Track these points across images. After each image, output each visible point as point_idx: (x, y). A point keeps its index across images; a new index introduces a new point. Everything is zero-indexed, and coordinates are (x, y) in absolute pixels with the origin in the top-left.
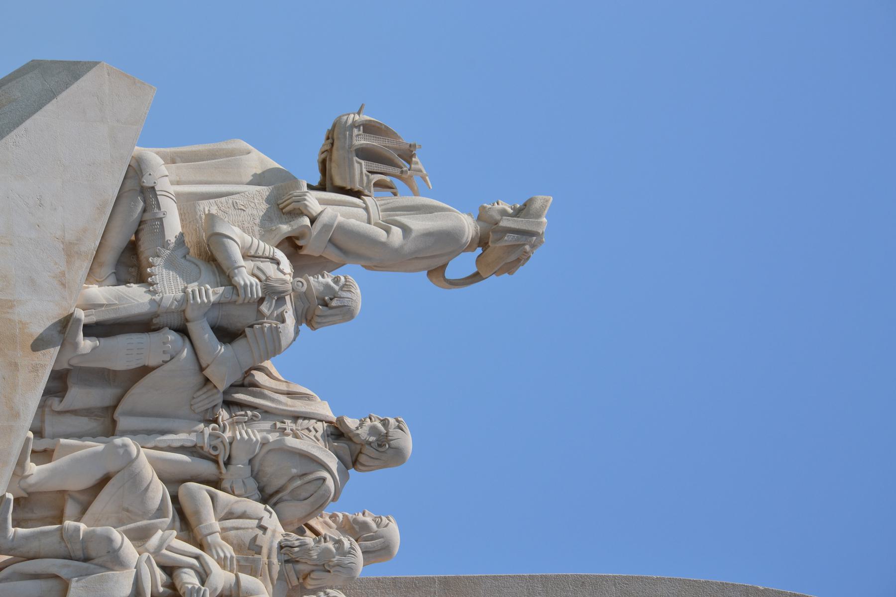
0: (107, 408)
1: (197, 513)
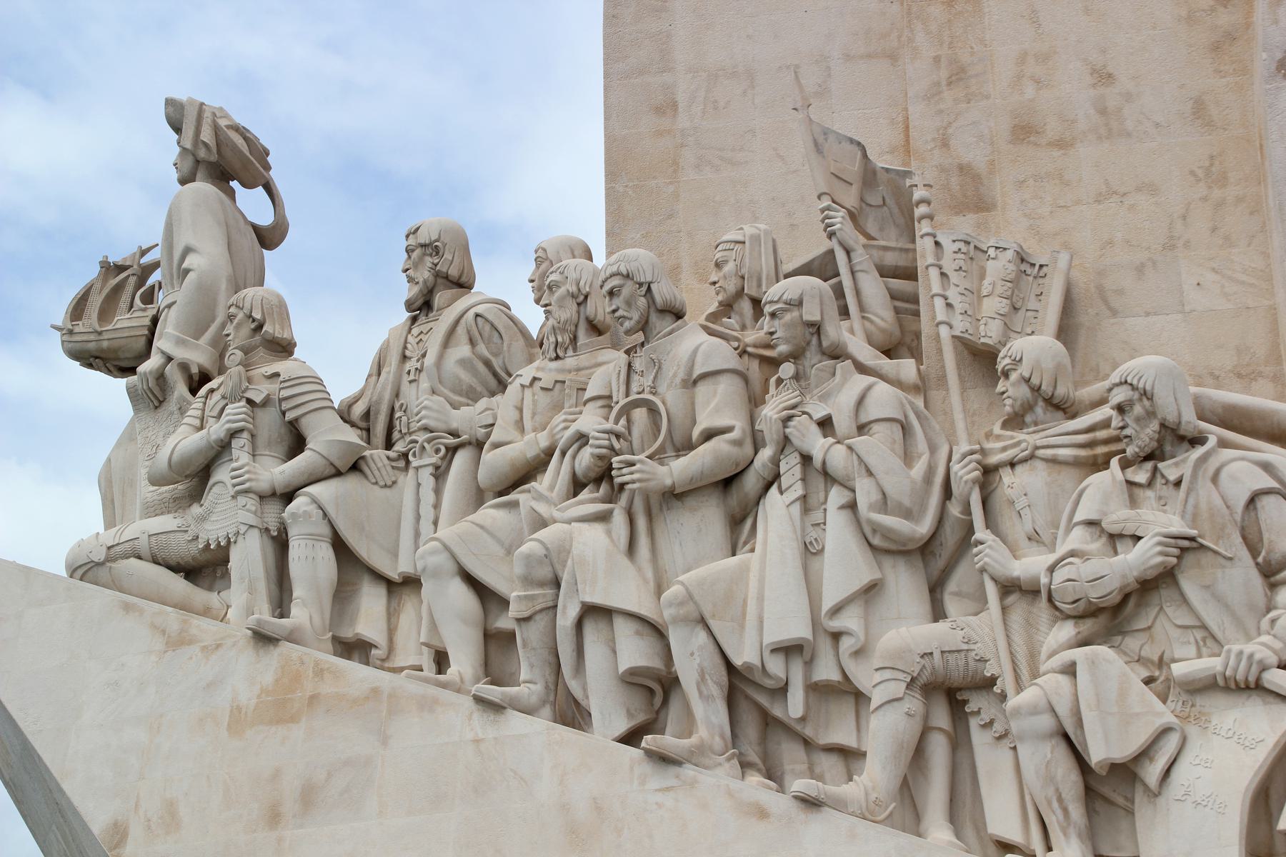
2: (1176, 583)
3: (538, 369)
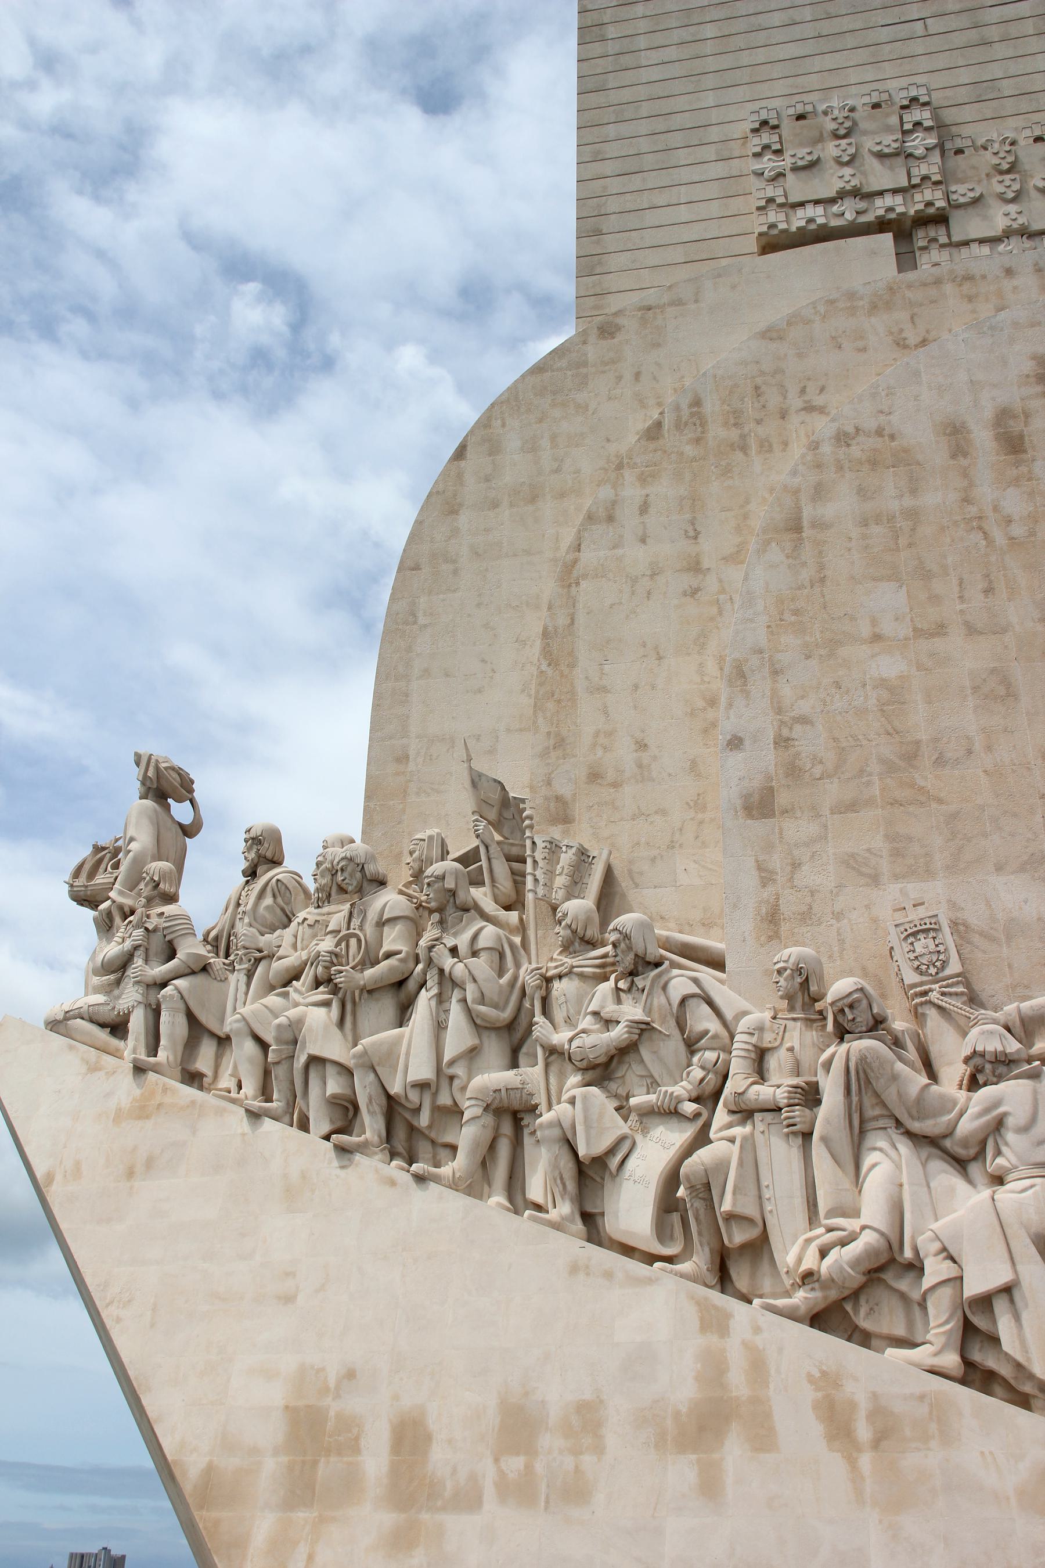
1: (287, 970)
2: (637, 1051)
3: (308, 913)
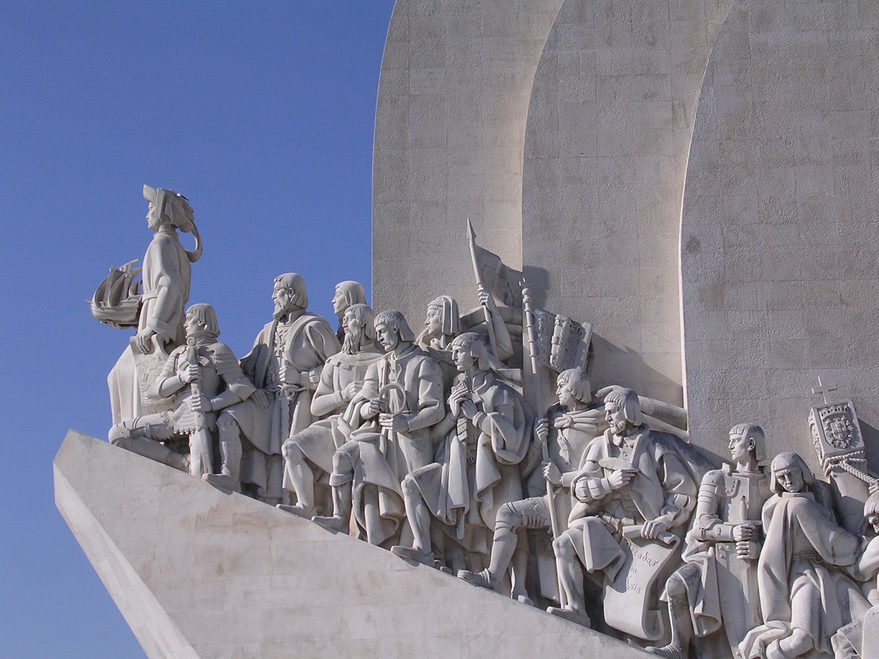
0: (265, 458)
